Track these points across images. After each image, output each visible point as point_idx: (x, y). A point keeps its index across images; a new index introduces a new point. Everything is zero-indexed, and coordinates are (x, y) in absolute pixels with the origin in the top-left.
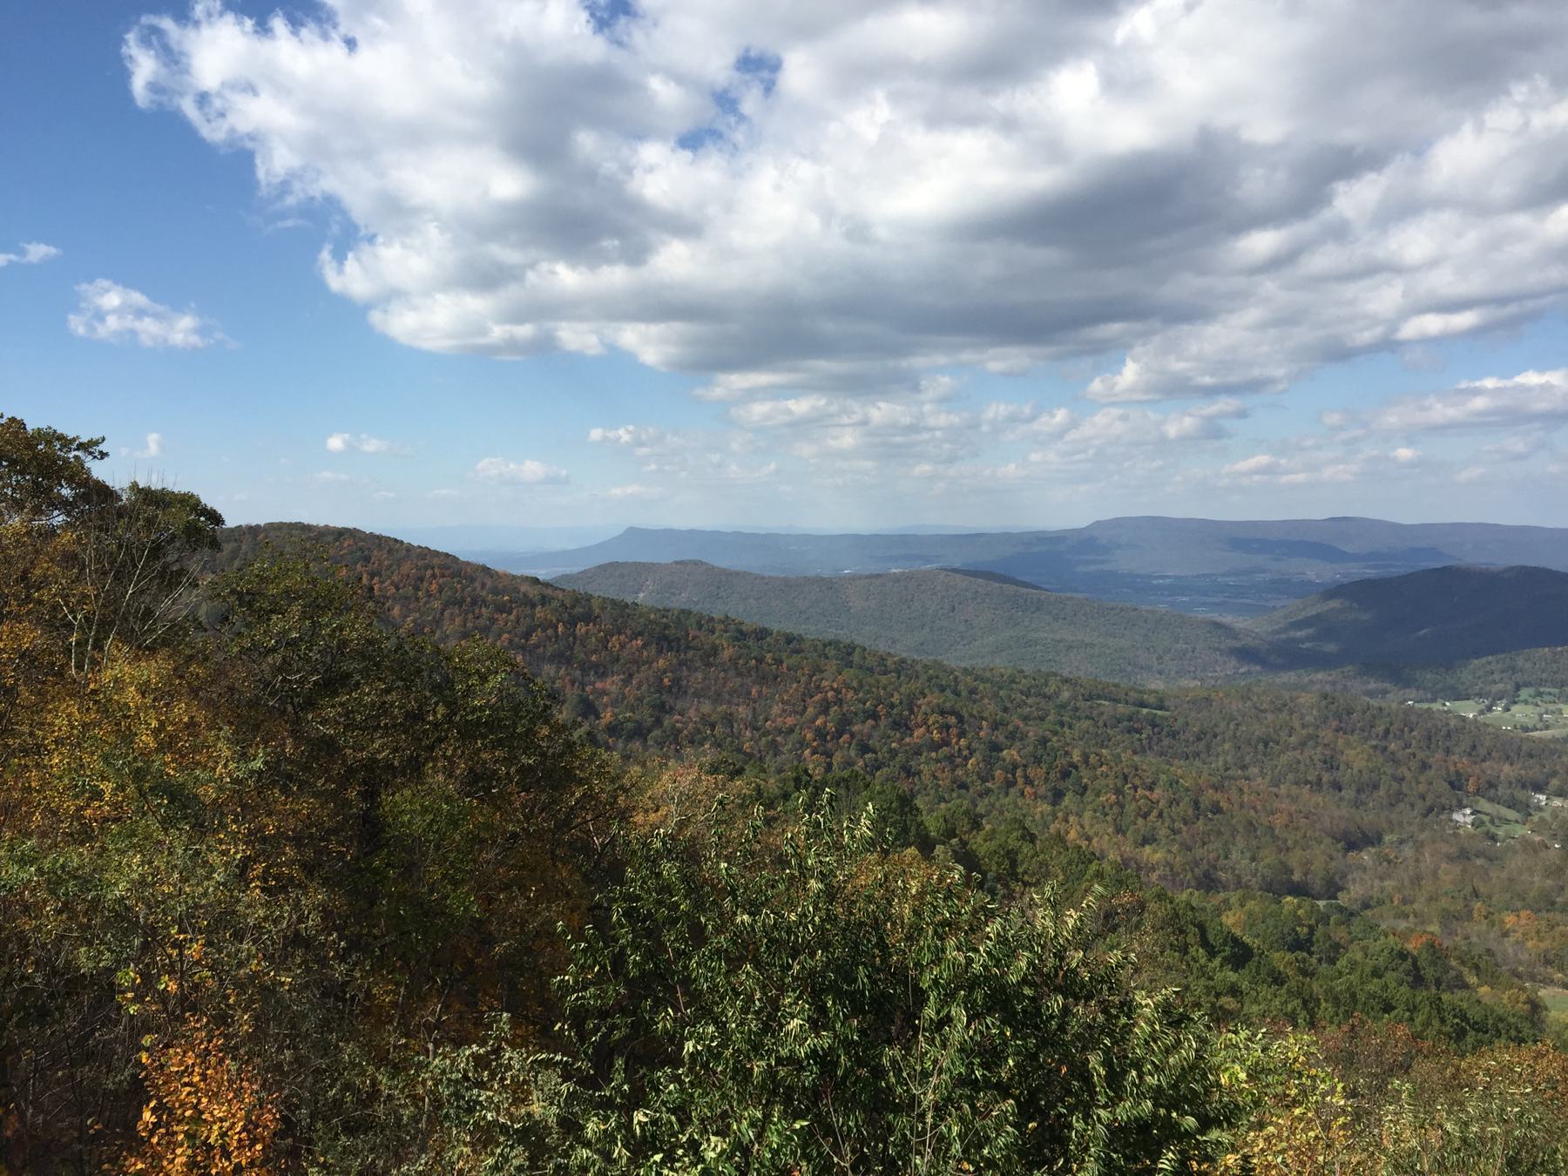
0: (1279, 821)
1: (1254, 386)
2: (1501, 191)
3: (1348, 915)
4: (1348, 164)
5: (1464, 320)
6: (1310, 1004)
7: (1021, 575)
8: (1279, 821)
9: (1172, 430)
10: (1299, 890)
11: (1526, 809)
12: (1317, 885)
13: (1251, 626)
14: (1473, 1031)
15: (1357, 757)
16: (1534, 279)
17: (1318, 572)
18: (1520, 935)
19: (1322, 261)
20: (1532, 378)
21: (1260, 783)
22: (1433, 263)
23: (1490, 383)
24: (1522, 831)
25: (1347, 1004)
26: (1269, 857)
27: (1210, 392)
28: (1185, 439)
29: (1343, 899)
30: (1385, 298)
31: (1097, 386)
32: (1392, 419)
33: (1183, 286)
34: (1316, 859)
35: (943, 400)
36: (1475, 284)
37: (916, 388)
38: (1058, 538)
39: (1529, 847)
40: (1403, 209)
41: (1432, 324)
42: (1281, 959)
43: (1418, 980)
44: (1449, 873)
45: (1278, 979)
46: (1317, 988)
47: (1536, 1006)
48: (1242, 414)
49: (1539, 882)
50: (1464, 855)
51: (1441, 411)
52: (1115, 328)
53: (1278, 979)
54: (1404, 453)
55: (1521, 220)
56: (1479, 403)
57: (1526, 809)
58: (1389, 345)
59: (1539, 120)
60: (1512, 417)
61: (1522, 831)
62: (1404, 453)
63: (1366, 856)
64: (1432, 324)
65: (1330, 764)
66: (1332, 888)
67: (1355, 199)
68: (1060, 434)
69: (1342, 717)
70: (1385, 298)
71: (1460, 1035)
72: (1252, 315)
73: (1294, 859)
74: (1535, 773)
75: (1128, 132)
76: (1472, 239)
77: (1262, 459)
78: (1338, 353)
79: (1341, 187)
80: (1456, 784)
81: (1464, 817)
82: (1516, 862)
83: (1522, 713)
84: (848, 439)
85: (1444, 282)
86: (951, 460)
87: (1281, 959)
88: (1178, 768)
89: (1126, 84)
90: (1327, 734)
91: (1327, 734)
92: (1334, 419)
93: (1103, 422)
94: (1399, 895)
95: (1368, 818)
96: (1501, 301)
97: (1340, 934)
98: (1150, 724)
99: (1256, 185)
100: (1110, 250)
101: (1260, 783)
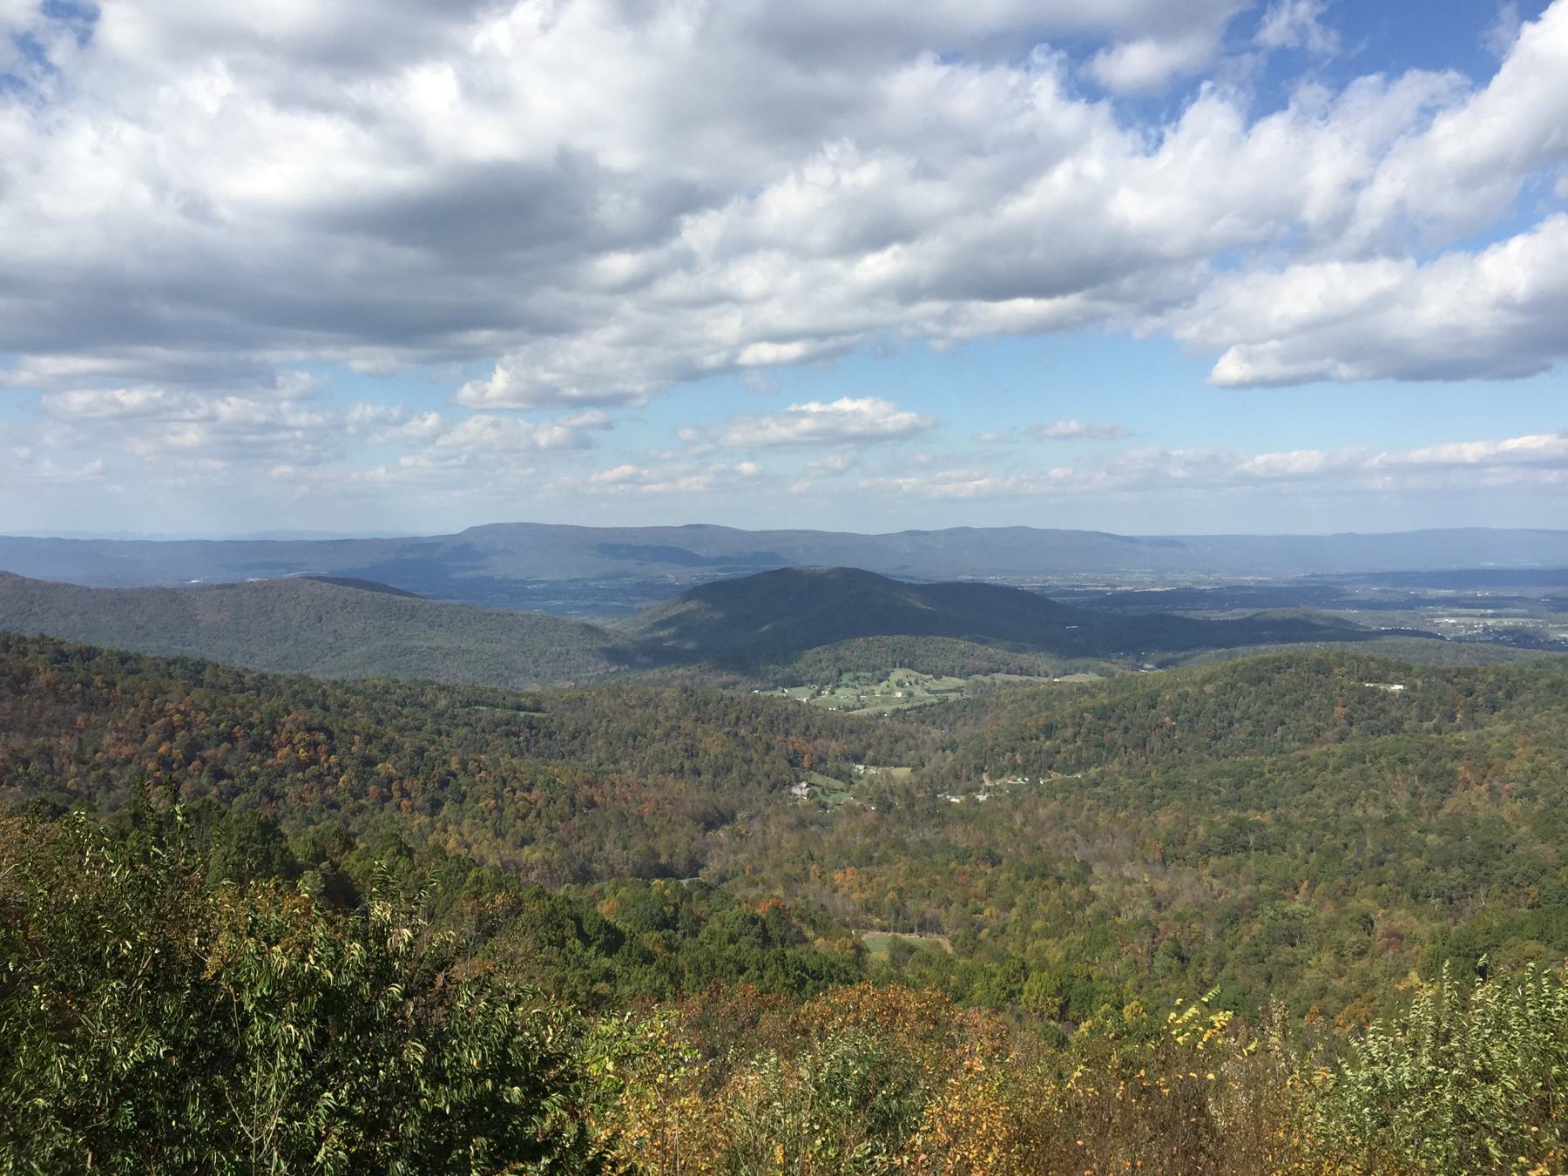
0: (647, 809)
1: (617, 400)
2: (820, 238)
3: (708, 889)
4: (692, 199)
5: (793, 350)
6: (676, 977)
7: (390, 582)
8: (647, 809)
9: (543, 439)
10: (665, 872)
11: (847, 777)
12: (681, 863)
13: (622, 627)
14: (811, 979)
15: (713, 744)
16: (846, 318)
17: (678, 575)
18: (846, 888)
19: (674, 286)
20: (846, 405)
22: (766, 298)
23: (814, 407)
24: (846, 798)
26: (639, 845)
27: (578, 404)
28: (554, 448)
29: (704, 876)
30: (726, 326)
31: (467, 391)
32: (736, 436)
33: (548, 300)
35: (306, 399)
36: (799, 319)
37: (271, 384)
38: (432, 544)
39: (854, 812)
40: (739, 247)
44: (790, 841)
45: (648, 958)
46: (682, 961)
47: (860, 950)
48: (608, 426)
49: (861, 841)
50: (802, 824)
51: (776, 431)
52: (484, 335)
53: (648, 958)
54: (747, 467)
55: (835, 266)
56: (806, 425)
57: (847, 777)
58: (731, 369)
60: (831, 438)
61: (846, 798)
62: (747, 467)
63: (722, 834)
64: (766, 352)
65: (691, 752)
66: (694, 867)
67: (701, 231)
68: (432, 439)
69: (699, 707)
70: (726, 326)
71: (802, 983)
72: (614, 332)
73: (661, 844)
74: (856, 746)
75: (488, 141)
76: (795, 280)
77: (627, 469)
78: (690, 374)
79: (687, 220)
80: (794, 762)
81: (801, 790)
82: (842, 825)
83: (844, 695)
84: (192, 436)
85: (774, 315)
86: (314, 462)
88: (555, 768)
89: (487, 92)
90: (687, 725)
91: (687, 725)
92: (687, 434)
93: (473, 429)
94: (749, 869)
95: (723, 799)
96: (821, 335)
97: (701, 908)
98: (527, 727)
99: (614, 210)
100: (471, 257)
101: (630, 775)
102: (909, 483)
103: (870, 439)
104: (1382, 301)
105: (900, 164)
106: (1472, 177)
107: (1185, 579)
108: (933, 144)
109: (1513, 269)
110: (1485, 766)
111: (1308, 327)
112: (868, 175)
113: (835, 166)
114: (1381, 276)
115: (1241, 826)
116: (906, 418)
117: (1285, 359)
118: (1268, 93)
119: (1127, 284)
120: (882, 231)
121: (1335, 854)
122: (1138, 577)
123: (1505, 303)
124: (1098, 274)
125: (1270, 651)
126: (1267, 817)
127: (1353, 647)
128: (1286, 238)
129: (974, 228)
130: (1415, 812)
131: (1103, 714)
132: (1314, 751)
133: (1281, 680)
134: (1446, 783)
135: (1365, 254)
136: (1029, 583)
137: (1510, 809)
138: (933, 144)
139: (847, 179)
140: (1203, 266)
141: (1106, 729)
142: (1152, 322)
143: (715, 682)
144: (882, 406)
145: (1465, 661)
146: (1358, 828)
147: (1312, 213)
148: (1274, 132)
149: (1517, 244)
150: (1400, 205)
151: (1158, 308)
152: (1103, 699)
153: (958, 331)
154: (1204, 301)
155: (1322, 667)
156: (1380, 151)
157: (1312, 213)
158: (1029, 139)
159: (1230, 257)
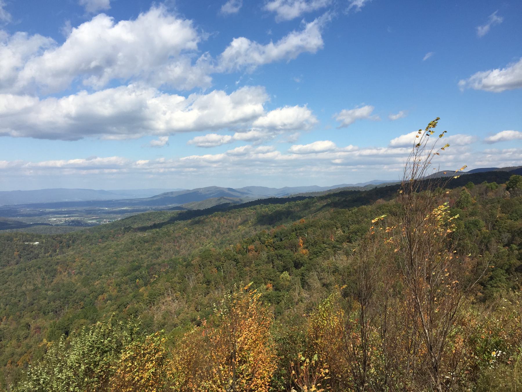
104: (27, 110)
106: (58, 74)
109: (70, 105)
114: (27, 102)
121: (16, 304)
123: (68, 116)
127: (21, 230)
130: (44, 284)
132: (6, 269)
134: (53, 273)
135: (21, 93)
145: (60, 232)
146: (24, 293)
149: (72, 98)
155: (9, 239)
156: (26, 59)
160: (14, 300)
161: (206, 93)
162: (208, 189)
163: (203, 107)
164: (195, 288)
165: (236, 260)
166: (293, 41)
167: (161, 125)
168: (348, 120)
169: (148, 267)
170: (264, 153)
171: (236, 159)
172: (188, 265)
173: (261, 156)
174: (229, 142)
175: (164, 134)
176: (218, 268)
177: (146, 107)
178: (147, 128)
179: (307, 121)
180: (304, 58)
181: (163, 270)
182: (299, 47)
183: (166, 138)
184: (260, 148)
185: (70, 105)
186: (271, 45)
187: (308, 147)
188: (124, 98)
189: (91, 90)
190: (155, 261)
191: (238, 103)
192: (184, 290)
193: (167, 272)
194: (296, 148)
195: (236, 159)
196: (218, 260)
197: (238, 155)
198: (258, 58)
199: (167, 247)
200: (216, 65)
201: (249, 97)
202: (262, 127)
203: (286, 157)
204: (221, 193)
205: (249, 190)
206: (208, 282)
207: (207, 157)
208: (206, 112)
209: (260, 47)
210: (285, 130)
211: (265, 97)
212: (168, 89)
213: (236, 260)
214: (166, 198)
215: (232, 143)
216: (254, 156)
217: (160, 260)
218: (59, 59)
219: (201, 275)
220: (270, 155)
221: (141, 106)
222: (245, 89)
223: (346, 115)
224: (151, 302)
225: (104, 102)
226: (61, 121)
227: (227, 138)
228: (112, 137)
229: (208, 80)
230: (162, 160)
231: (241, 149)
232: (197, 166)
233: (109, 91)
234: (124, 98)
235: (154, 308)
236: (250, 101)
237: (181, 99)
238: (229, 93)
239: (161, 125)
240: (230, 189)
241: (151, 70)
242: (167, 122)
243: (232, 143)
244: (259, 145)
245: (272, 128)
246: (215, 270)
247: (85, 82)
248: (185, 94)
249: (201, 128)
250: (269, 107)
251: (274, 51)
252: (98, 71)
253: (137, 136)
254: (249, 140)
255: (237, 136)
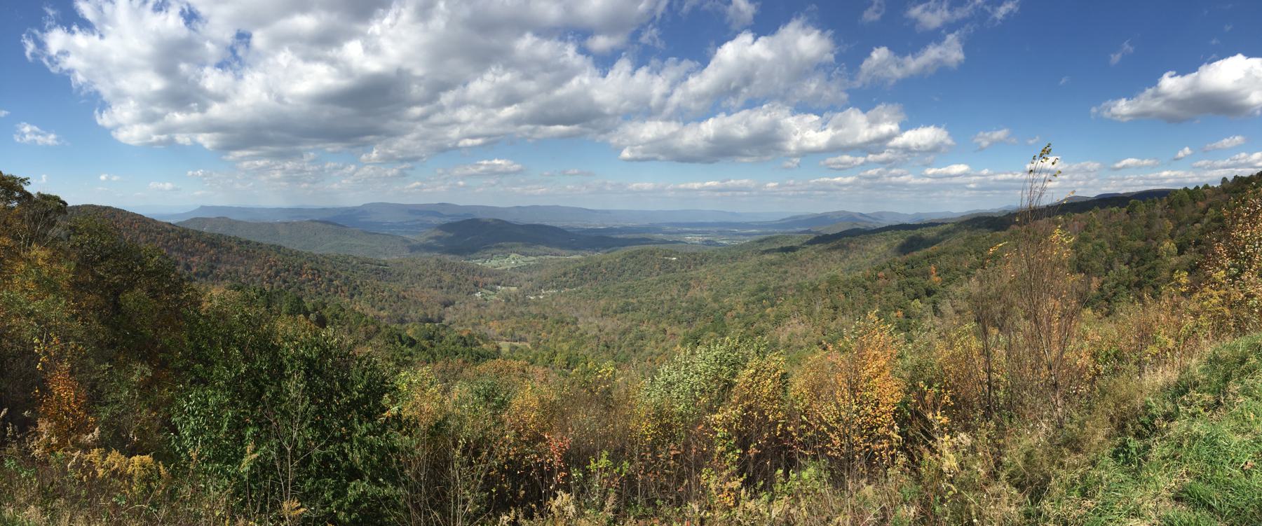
0: (424, 300)
1: (416, 159)
2: (489, 101)
3: (445, 327)
4: (445, 87)
5: (479, 141)
6: (433, 355)
7: (338, 222)
8: (424, 300)
9: (389, 173)
10: (430, 321)
11: (494, 290)
12: (436, 318)
13: (419, 238)
14: (480, 357)
15: (447, 278)
16: (495, 130)
17: (435, 221)
18: (494, 328)
19: (438, 118)
20: (497, 162)
21: (418, 288)
22: (469, 122)
23: (485, 162)
24: (495, 297)
25: (446, 354)
26: (421, 312)
27: (402, 161)
28: (393, 176)
29: (444, 322)
30: (455, 133)
31: (364, 157)
32: (457, 172)
33: (392, 124)
34: (435, 311)
35: (312, 162)
36: (480, 130)
37: (302, 157)
38: (354, 209)
39: (497, 302)
40: (460, 104)
41: (469, 142)
42: (425, 343)
43: (465, 344)
44: (475, 311)
45: (424, 349)
46: (435, 350)
47: (498, 348)
48: (412, 169)
49: (499, 311)
50: (478, 306)
51: (473, 170)
52: (371, 138)
53: (424, 349)
54: (461, 183)
55: (494, 111)
56: (482, 168)
57: (494, 290)
58: (456, 148)
59: (498, 79)
60: (492, 173)
61: (495, 297)
62: (461, 183)
63: (450, 309)
64: (469, 142)
65: (439, 281)
66: (440, 319)
67: (447, 98)
68: (352, 174)
69: (442, 265)
70: (455, 133)
71: (478, 359)
72: (415, 135)
73: (429, 312)
74: (498, 280)
75: (373, 66)
76: (480, 115)
77: (418, 183)
78: (442, 150)
79: (442, 94)
80: (476, 285)
81: (478, 295)
82: (493, 306)
83: (494, 263)
84: (278, 175)
85: (471, 128)
86: (314, 182)
87: (425, 343)
88: (392, 285)
89: (373, 49)
90: (438, 272)
91: (438, 272)
92: (440, 171)
93: (367, 170)
94: (460, 320)
95: (451, 297)
96: (489, 136)
97: (443, 333)
98: (382, 271)
99: (417, 90)
100: (369, 106)
101: (418, 288)
102: (518, 189)
103: (506, 173)
104: (673, 135)
105: (518, 74)
106: (699, 97)
107: (610, 224)
108: (527, 67)
109: (710, 128)
110: (699, 281)
111: (651, 142)
112: (507, 77)
113: (495, 74)
114: (673, 127)
115: (627, 304)
116: (517, 167)
117: (644, 152)
118: (640, 61)
119: (594, 122)
120: (510, 98)
121: (655, 311)
122: (596, 223)
123: (707, 139)
124: (586, 118)
125: (636, 248)
126: (635, 301)
127: (661, 246)
128: (644, 110)
129: (543, 99)
130: (679, 296)
131: (583, 269)
132: (649, 279)
133: (641, 257)
134: (688, 287)
135: (668, 119)
136: (559, 225)
137: (706, 294)
138: (527, 67)
139: (498, 79)
140: (619, 118)
141: (584, 274)
142: (603, 137)
143: (448, 258)
144: (510, 162)
145: (694, 250)
146: (662, 302)
147: (654, 102)
148: (642, 74)
149: (711, 121)
150: (679, 104)
151: (605, 131)
152: (583, 264)
153: (537, 136)
154: (620, 129)
155: (652, 253)
156: (674, 85)
157: (654, 102)
158: (563, 67)
159: (628, 116)
160: (654, 307)
161: (842, 110)
162: (838, 213)
163: (838, 127)
164: (822, 312)
165: (864, 287)
166: (932, 53)
167: (792, 146)
168: (985, 143)
169: (774, 289)
170: (897, 176)
171: (868, 182)
172: (815, 289)
173: (893, 179)
174: (862, 164)
175: (796, 156)
176: (846, 294)
177: (779, 127)
178: (780, 150)
179: (942, 143)
180: (942, 72)
181: (789, 293)
182: (938, 61)
183: (797, 160)
184: (894, 171)
185: (710, 128)
186: (909, 58)
187: (944, 170)
188: (760, 119)
189: (729, 113)
190: (781, 284)
191: (874, 122)
192: (810, 314)
193: (793, 295)
194: (930, 171)
195: (868, 182)
196: (846, 286)
197: (872, 178)
198: (897, 73)
199: (794, 270)
200: (851, 79)
201: (885, 116)
202: (896, 148)
203: (919, 181)
204: (851, 217)
205: (881, 214)
206: (836, 308)
207: (838, 179)
208: (839, 132)
209: (898, 58)
210: (920, 152)
211: (902, 117)
212: (802, 108)
213: (864, 287)
214: (796, 221)
215: (866, 165)
216: (886, 179)
217: (786, 283)
218: (703, 82)
219: (828, 300)
220: (903, 178)
221: (775, 125)
222: (881, 107)
223: (984, 138)
224: (778, 322)
225: (739, 124)
226: (701, 145)
227: (861, 160)
228: (745, 160)
229: (844, 96)
230: (792, 182)
231: (872, 172)
232: (826, 188)
233: (744, 113)
234: (760, 119)
235: (780, 329)
236: (887, 121)
237: (816, 118)
238: (864, 111)
239: (792, 146)
240: (861, 215)
241: (788, 88)
242: (798, 143)
243: (866, 165)
244: (891, 168)
245: (906, 149)
246: (842, 296)
247: (724, 104)
248: (819, 112)
249: (835, 149)
250: (904, 127)
251: (913, 64)
252: (735, 92)
253: (769, 158)
254: (882, 163)
255: (870, 157)
